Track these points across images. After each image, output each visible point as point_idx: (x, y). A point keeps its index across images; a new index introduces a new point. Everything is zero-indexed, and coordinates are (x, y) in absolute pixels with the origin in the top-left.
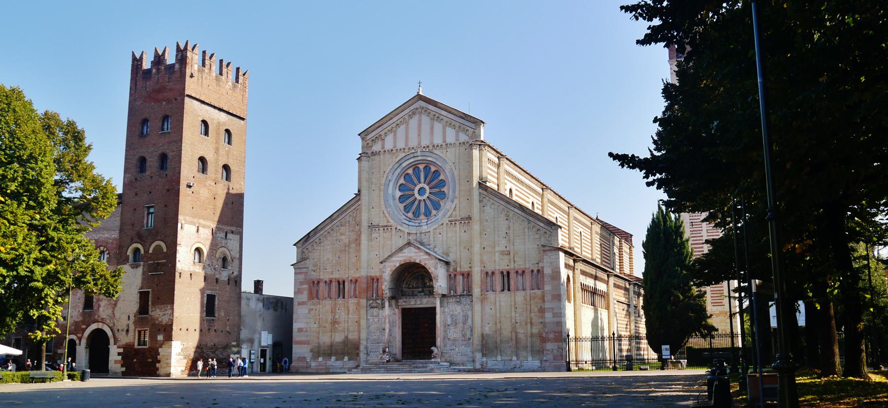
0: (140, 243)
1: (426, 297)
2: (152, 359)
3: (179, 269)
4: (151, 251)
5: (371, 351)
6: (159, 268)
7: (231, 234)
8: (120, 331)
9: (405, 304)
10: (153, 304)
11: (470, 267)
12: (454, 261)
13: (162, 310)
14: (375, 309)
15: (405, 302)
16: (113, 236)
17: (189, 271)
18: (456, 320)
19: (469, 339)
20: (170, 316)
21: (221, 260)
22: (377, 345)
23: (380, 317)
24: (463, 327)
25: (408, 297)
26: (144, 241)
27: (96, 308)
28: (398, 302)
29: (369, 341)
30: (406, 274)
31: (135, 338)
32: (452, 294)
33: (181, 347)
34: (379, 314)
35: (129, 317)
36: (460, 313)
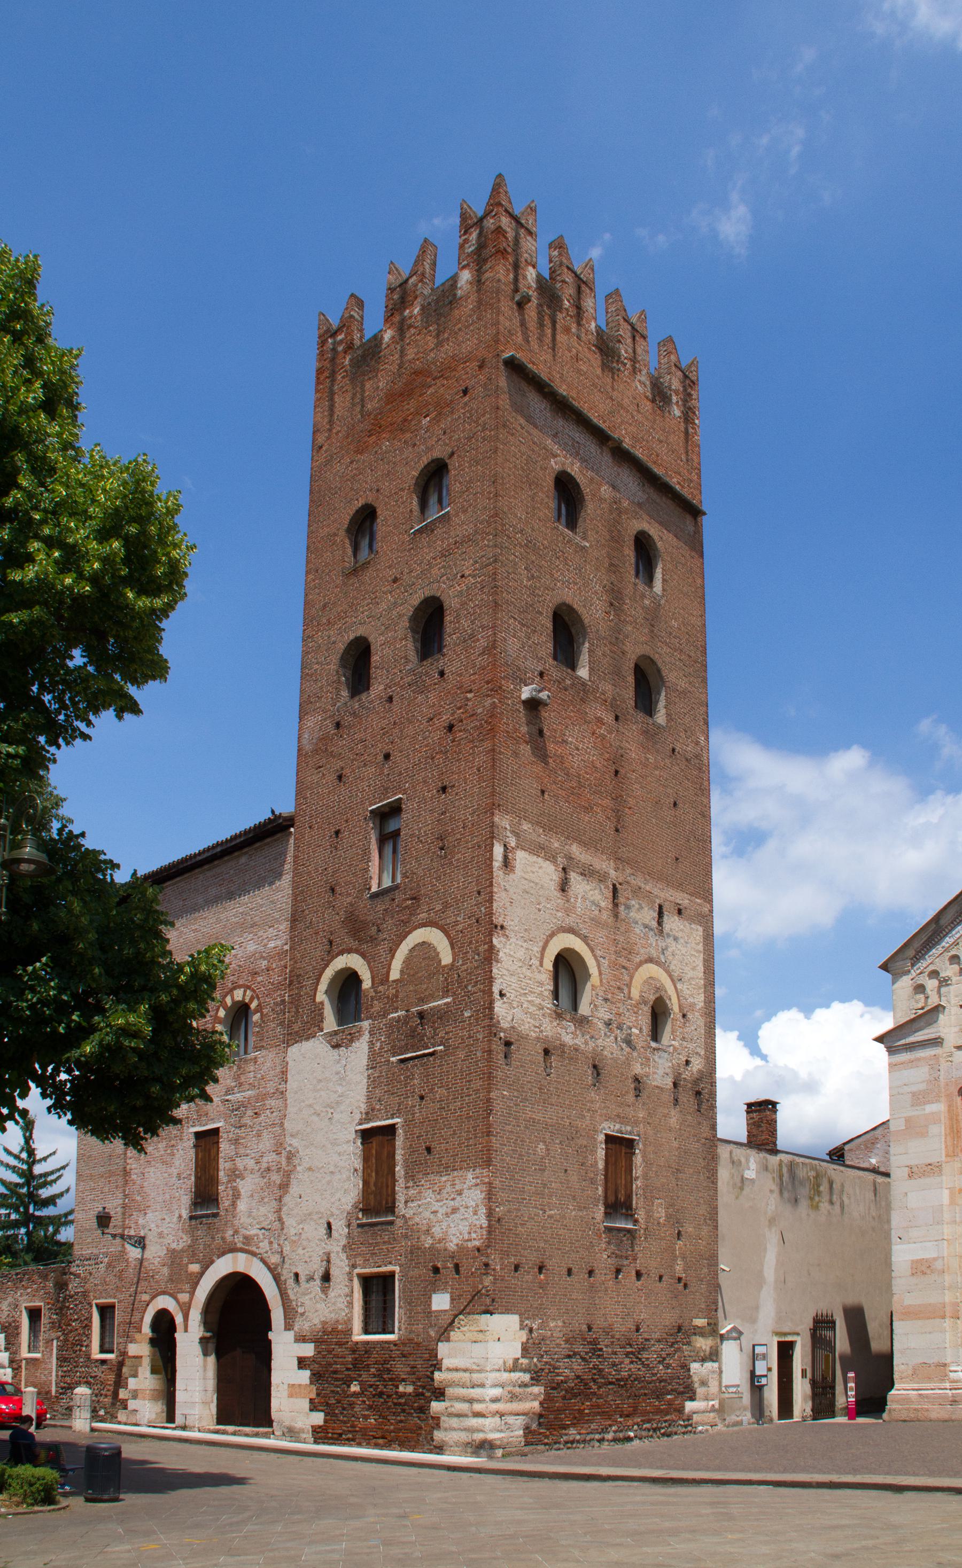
0: (357, 951)
2: (414, 1383)
3: (505, 1025)
4: (395, 975)
6: (429, 1031)
7: (676, 918)
8: (302, 1278)
10: (410, 1176)
13: (444, 1195)
16: (272, 945)
17: (538, 1038)
20: (475, 1213)
21: (647, 1009)
26: (373, 939)
27: (227, 1203)
31: (350, 1304)
33: (523, 1336)
35: (329, 1225)
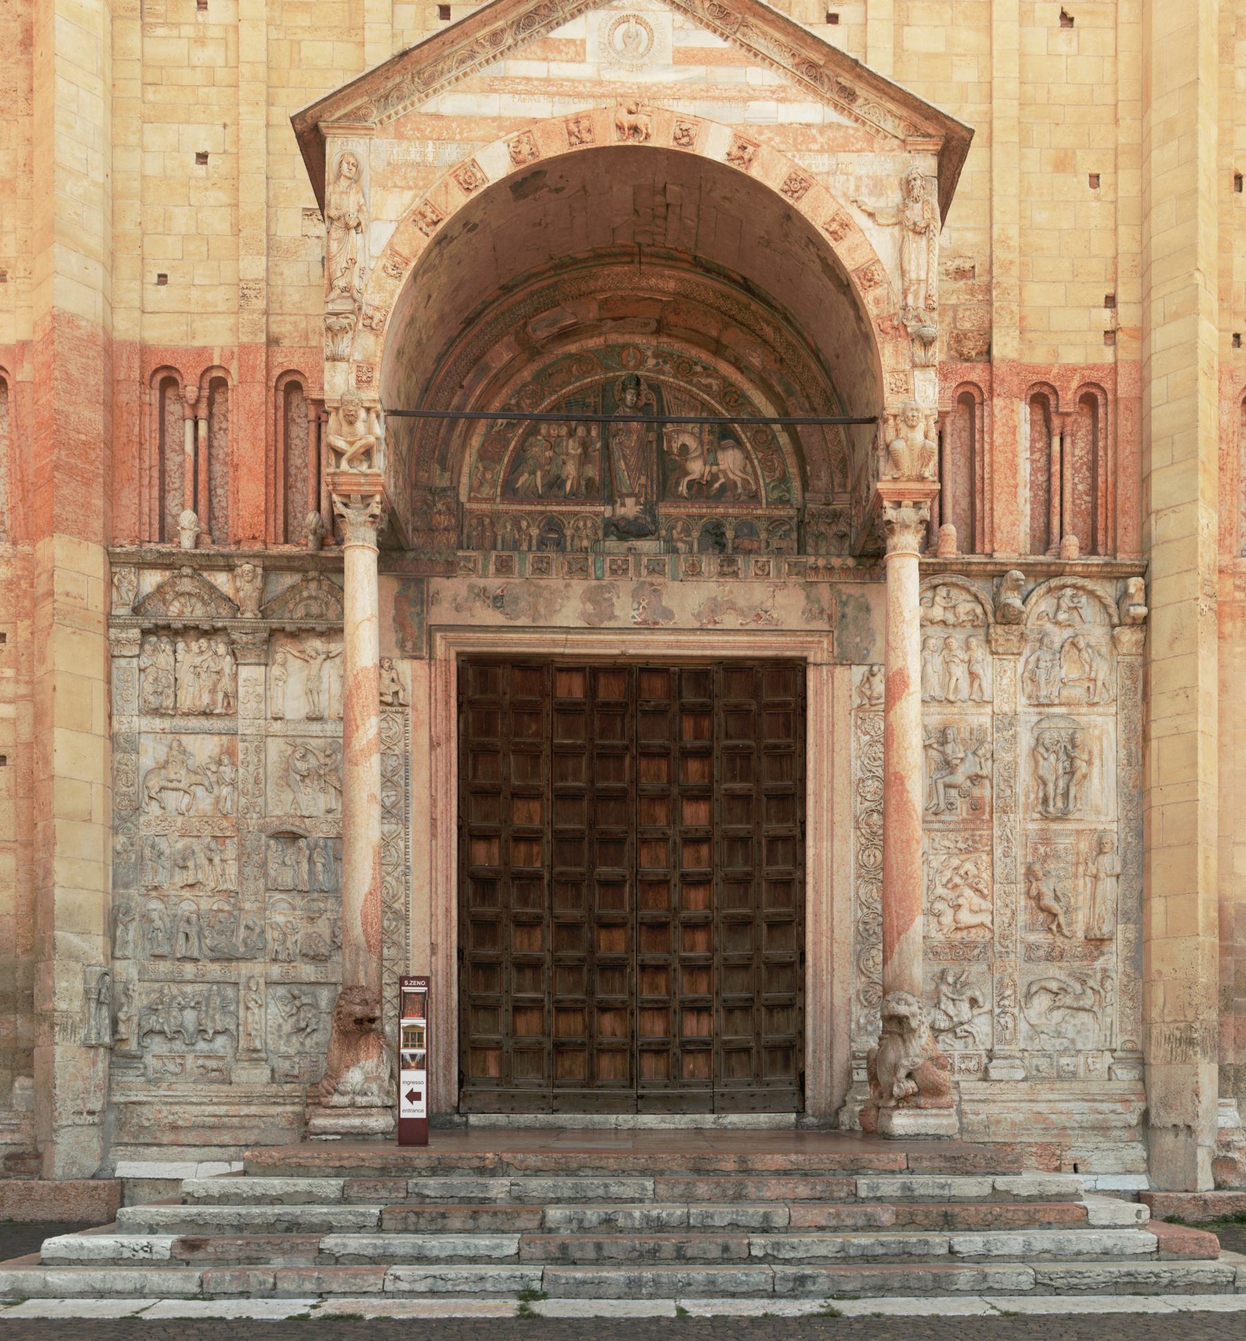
1: (694, 572)
5: (153, 1022)
9: (493, 617)
11: (1110, 335)
12: (960, 274)
14: (191, 653)
15: (498, 601)
18: (975, 779)
19: (1097, 943)
22: (215, 970)
23: (244, 726)
24: (1045, 838)
25: (525, 563)
28: (434, 599)
29: (131, 933)
30: (502, 355)
32: (950, 548)
34: (230, 698)
36: (1010, 721)
